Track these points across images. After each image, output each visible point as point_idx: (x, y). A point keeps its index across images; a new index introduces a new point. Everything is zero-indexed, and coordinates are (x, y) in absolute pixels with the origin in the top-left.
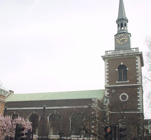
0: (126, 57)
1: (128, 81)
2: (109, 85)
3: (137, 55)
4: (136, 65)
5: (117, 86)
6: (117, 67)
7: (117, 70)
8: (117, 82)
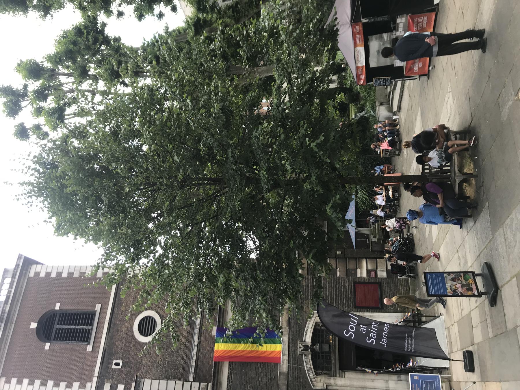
0: (18, 310)
1: (98, 307)
2: (91, 381)
3: (27, 270)
4: (55, 276)
5: (104, 351)
6: (41, 343)
7: (47, 346)
8: (89, 348)
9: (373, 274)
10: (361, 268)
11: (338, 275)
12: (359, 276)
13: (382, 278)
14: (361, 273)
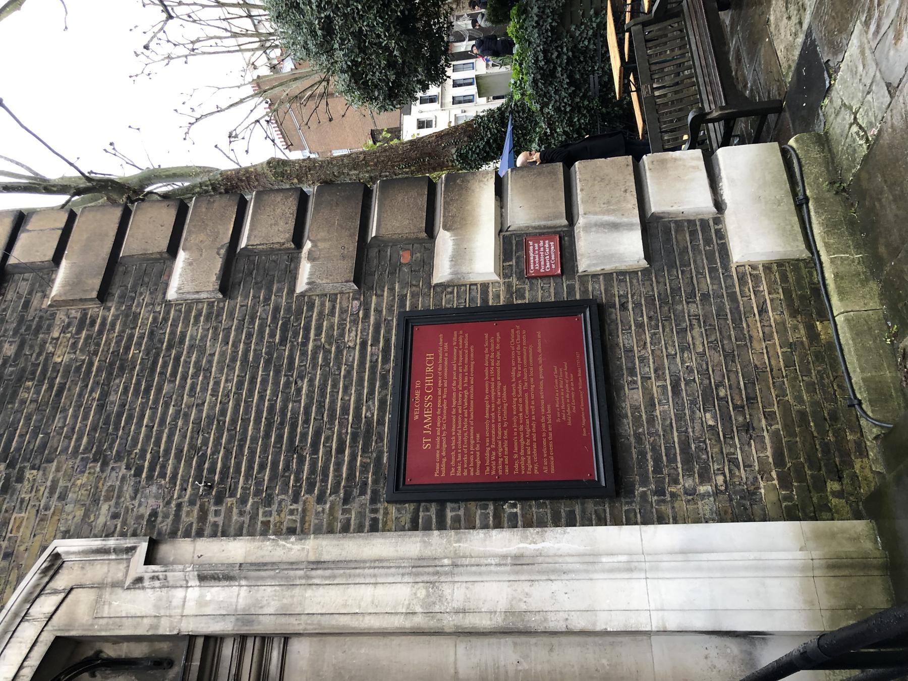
9: (542, 258)
10: (459, 223)
11: (301, 286)
12: (442, 272)
13: (608, 276)
14: (460, 255)
